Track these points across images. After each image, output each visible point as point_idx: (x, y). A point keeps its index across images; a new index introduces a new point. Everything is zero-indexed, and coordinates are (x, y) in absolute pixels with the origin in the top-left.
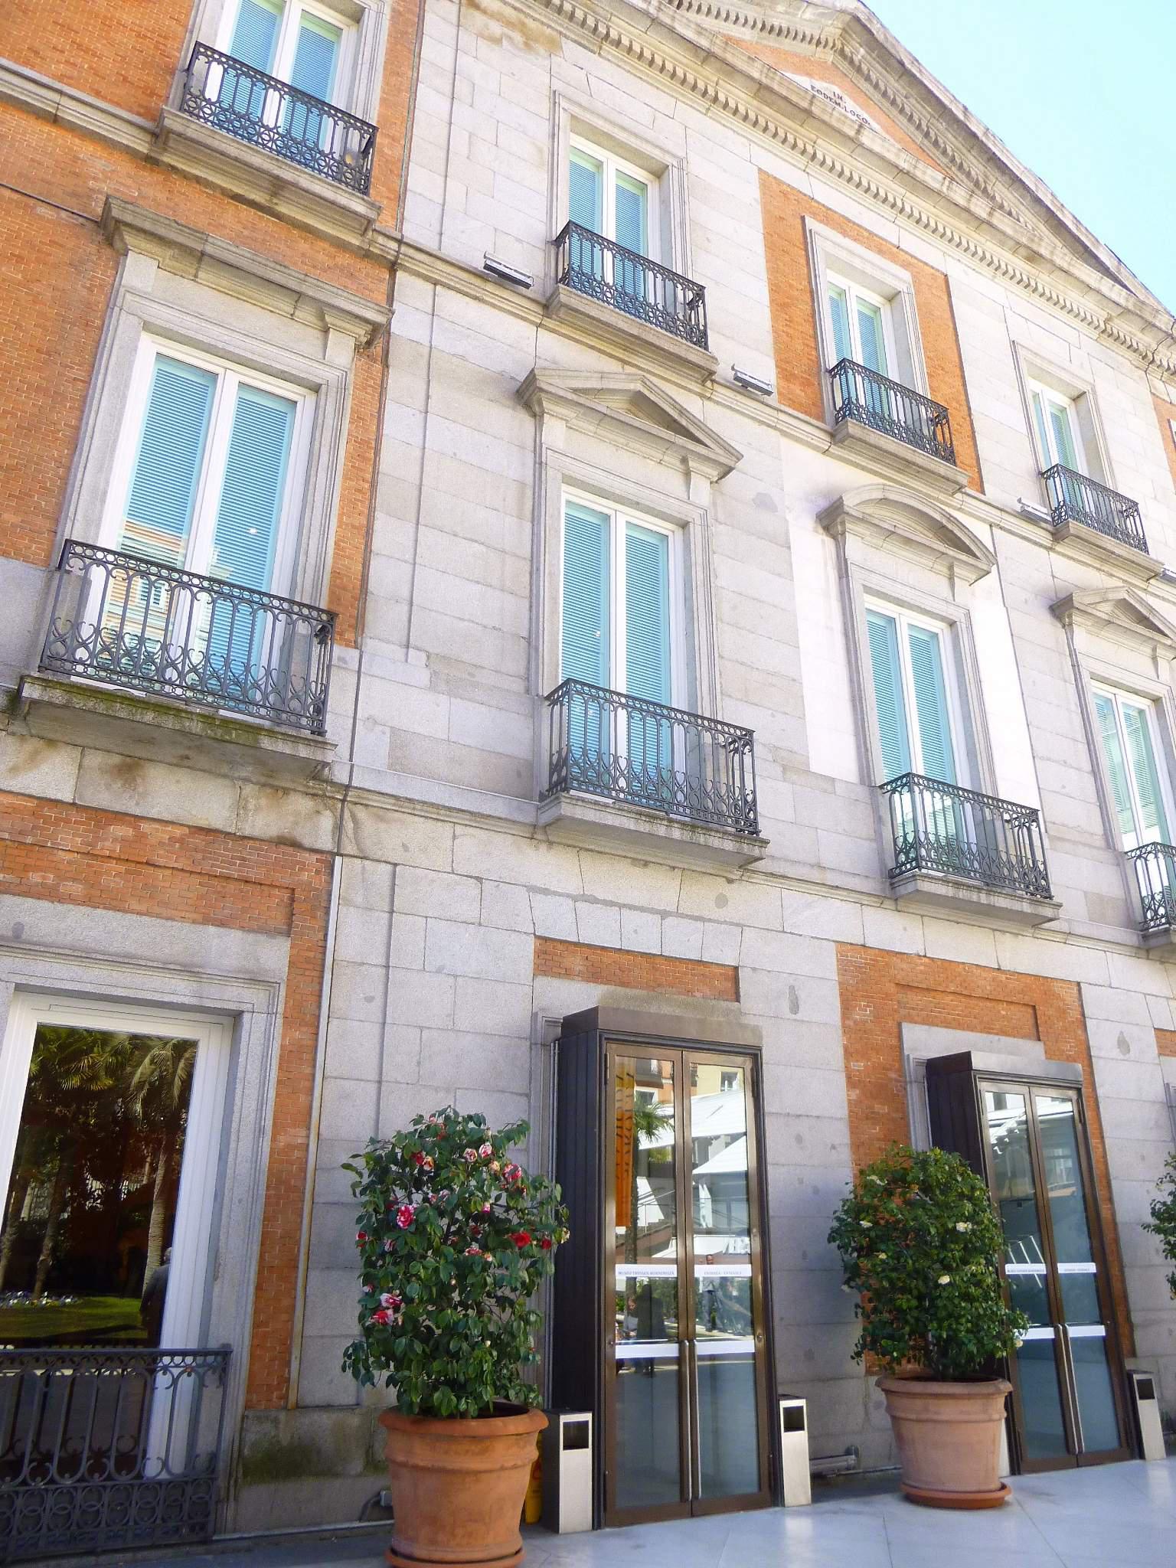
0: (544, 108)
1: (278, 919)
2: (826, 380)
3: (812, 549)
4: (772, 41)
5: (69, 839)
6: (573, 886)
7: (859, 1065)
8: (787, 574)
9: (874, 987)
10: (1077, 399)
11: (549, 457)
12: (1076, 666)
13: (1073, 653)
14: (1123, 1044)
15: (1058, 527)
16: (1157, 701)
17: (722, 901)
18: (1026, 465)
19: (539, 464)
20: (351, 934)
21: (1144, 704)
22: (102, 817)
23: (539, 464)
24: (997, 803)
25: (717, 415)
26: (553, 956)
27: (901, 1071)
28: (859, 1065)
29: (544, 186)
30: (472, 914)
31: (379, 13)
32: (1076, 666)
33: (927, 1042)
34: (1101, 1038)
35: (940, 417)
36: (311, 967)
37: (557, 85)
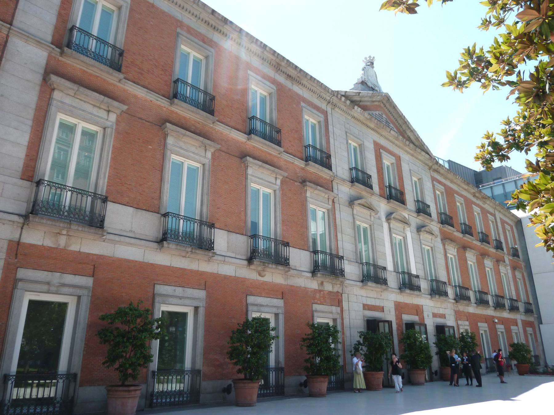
0: (345, 137)
1: (337, 305)
3: (385, 225)
5: (318, 296)
6: (365, 295)
8: (383, 232)
9: (400, 308)
10: (419, 179)
11: (355, 216)
12: (421, 243)
13: (420, 240)
14: (428, 316)
16: (432, 248)
17: (381, 295)
19: (354, 218)
21: (429, 248)
22: (320, 291)
23: (354, 218)
26: (366, 307)
29: (347, 156)
32: (421, 243)
36: (342, 311)
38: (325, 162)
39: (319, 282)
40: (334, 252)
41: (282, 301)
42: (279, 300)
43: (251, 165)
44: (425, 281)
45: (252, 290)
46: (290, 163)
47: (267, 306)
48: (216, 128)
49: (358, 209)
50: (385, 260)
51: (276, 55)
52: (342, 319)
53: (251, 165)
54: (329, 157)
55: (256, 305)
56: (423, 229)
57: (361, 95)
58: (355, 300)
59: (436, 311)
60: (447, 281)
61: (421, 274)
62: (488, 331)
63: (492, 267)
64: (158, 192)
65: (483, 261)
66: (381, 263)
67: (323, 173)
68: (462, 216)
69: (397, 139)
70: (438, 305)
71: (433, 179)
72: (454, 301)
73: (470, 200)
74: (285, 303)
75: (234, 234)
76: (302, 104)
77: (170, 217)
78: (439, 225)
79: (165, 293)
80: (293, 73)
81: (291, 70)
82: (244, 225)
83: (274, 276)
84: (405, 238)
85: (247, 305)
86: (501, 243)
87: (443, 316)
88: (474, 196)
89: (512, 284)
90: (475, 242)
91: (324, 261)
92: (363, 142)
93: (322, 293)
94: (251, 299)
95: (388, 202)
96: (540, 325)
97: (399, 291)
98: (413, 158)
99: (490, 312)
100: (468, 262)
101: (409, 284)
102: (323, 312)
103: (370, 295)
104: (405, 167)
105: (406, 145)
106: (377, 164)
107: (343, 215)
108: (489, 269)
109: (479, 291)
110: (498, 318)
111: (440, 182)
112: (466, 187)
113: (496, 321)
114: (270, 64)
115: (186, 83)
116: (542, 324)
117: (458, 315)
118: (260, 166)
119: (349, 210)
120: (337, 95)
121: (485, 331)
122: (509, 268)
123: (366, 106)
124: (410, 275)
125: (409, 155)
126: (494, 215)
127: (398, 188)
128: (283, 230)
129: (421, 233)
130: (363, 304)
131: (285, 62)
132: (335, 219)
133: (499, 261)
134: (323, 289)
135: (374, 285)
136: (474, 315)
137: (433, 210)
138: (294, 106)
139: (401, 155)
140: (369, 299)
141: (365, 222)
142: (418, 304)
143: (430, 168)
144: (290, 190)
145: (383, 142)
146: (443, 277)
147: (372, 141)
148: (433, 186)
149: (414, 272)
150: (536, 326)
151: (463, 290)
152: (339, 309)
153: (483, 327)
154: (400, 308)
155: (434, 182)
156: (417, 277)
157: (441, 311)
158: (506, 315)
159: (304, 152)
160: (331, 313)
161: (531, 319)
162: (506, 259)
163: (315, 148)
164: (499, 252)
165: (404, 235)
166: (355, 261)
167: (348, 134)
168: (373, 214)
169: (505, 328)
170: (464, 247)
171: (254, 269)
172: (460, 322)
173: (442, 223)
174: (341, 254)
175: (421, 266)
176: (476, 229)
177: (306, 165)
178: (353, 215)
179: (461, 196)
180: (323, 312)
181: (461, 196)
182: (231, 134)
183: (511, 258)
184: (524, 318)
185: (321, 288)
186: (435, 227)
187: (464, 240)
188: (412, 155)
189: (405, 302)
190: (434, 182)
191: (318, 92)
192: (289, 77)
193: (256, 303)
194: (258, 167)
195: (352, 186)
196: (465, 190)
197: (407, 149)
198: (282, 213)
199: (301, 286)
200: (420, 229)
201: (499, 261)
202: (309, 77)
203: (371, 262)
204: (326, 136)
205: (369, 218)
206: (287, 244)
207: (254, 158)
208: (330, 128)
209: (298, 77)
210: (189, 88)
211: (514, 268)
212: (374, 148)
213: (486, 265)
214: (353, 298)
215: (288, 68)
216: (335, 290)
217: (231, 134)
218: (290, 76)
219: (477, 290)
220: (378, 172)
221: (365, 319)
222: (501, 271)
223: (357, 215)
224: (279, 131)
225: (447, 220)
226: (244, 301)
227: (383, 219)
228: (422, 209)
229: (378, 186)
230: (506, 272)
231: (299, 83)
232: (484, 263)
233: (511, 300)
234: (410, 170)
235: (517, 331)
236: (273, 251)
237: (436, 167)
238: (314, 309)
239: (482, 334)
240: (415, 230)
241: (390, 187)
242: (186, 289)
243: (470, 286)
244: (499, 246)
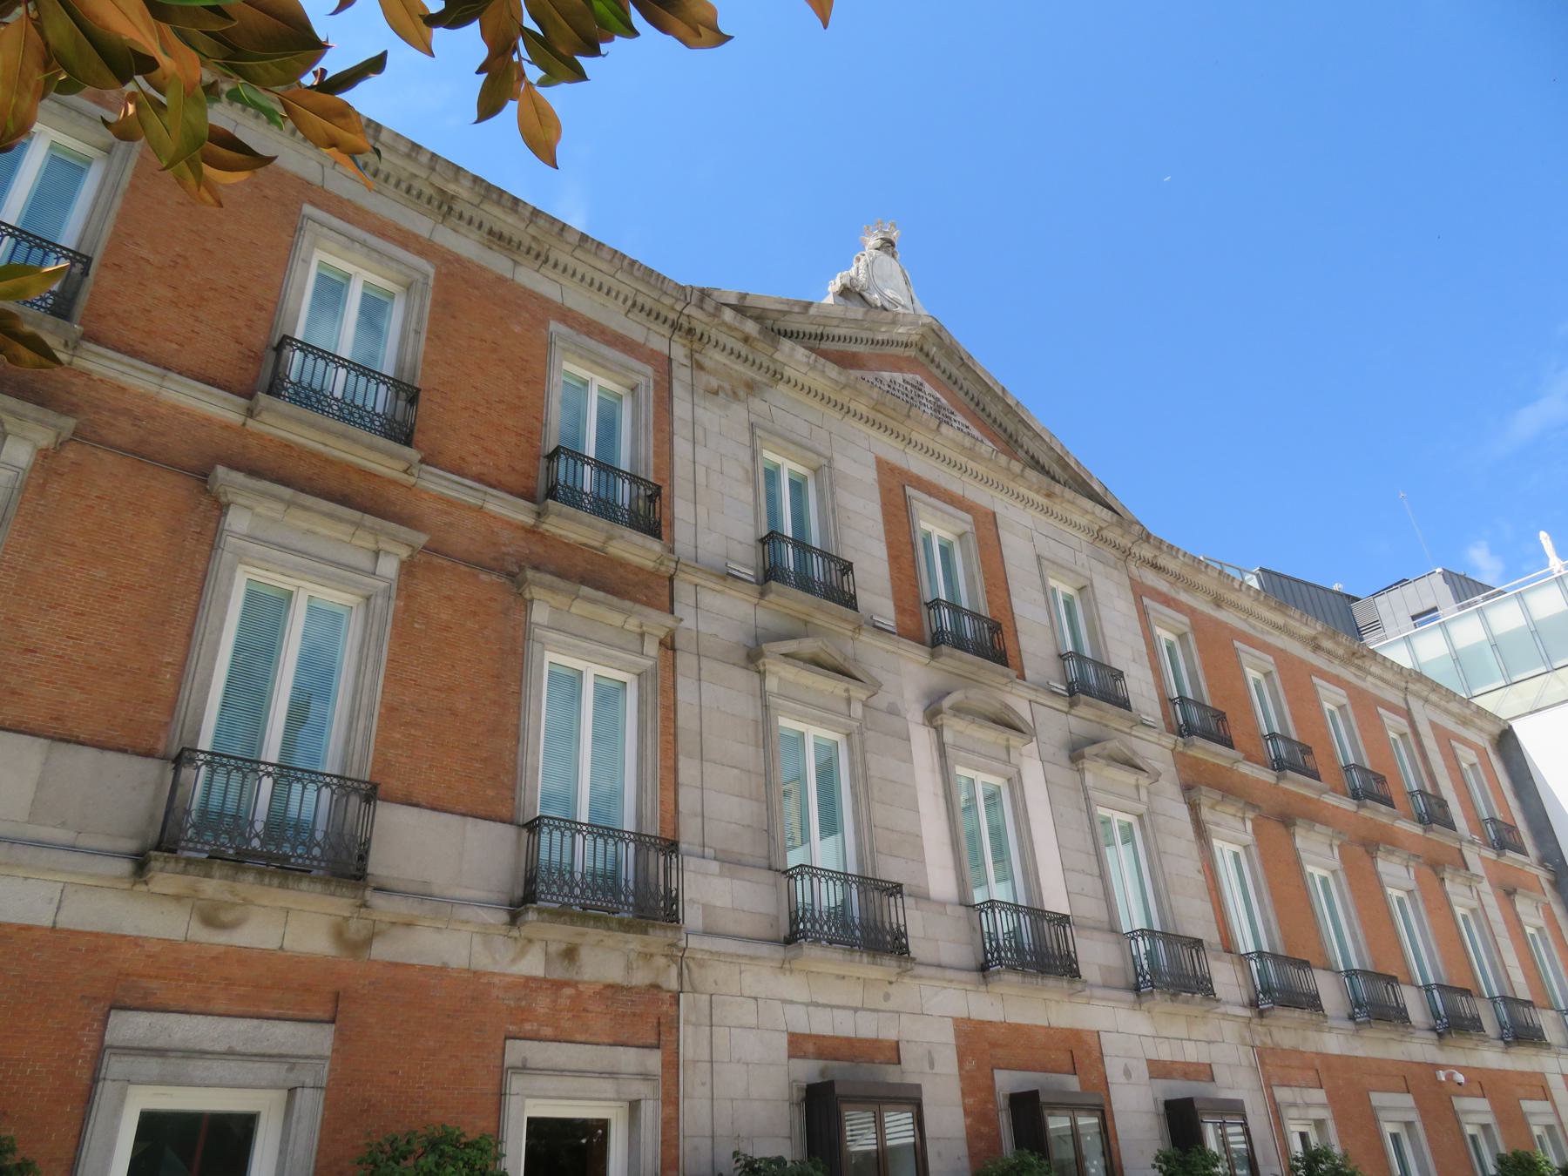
0: (746, 438)
2: (924, 610)
3: (922, 738)
4: (878, 350)
5: (542, 1004)
6: (805, 998)
7: (970, 1101)
8: (908, 759)
9: (977, 1043)
10: (1081, 590)
12: (1087, 799)
13: (1085, 789)
14: (1127, 1073)
15: (1075, 691)
16: (1140, 817)
17: (887, 997)
18: (1048, 650)
20: (691, 1042)
22: (558, 985)
26: (798, 1045)
27: (995, 1102)
28: (970, 1101)
29: (751, 499)
30: (752, 1021)
31: (648, 387)
33: (1007, 1082)
34: (1114, 1069)
35: (996, 628)
36: (672, 1065)
37: (753, 418)
38: (650, 515)
39: (553, 948)
43: (240, 500)
44: (1111, 937)
45: (154, 984)
46: (470, 507)
47: (230, 1054)
48: (89, 366)
49: (780, 674)
51: (424, 159)
53: (240, 500)
55: (160, 1053)
56: (1088, 750)
57: (812, 311)
58: (751, 1020)
59: (1165, 1053)
60: (1210, 935)
62: (1419, 1126)
63: (1412, 885)
65: (1374, 866)
66: (891, 870)
67: (634, 549)
68: (1268, 712)
69: (971, 453)
70: (1178, 1028)
71: (1140, 592)
72: (1247, 1013)
73: (1302, 662)
74: (341, 1039)
75: (89, 754)
76: (554, 326)
78: (1169, 740)
80: (507, 223)
81: (497, 211)
83: (291, 924)
84: (1015, 783)
86: (1443, 804)
88: (1317, 648)
89: (1505, 943)
90: (1329, 799)
92: (830, 460)
93: (568, 991)
95: (933, 656)
97: (975, 976)
98: (1051, 520)
99: (1420, 1049)
100: (1389, 891)
101: (1038, 950)
102: (560, 1072)
103: (836, 999)
104: (1017, 550)
105: (1015, 477)
106: (888, 532)
107: (713, 699)
108: (1401, 894)
109: (1440, 987)
111: (1168, 601)
112: (1279, 619)
114: (408, 191)
117: (1275, 1066)
118: (290, 504)
119: (743, 678)
120: (702, 300)
121: (1485, 1127)
122: (1485, 887)
123: (854, 355)
125: (1031, 511)
126: (1408, 714)
129: (1087, 764)
131: (467, 183)
133: (1437, 866)
134: (571, 975)
135: (1013, 978)
136: (1347, 1062)
137: (1139, 685)
139: (999, 509)
141: (821, 722)
142: (1078, 1026)
143: (1127, 553)
145: (917, 464)
146: (1195, 920)
147: (872, 461)
148: (1143, 614)
149: (1056, 902)
151: (1292, 972)
152: (654, 1061)
153: (1395, 1111)
154: (977, 1043)
155: (1146, 601)
157: (1192, 1053)
158: (1491, 1057)
160: (612, 1075)
162: (1471, 855)
164: (1438, 835)
165: (1012, 771)
166: (764, 863)
167: (758, 432)
168: (858, 693)
169: (1497, 1109)
170: (1282, 819)
171: (177, 898)
172: (1282, 1094)
173: (1185, 731)
176: (1332, 755)
177: (250, 413)
178: (763, 694)
179: (1265, 647)
180: (560, 1072)
181: (1265, 647)
182: (164, 392)
183: (1490, 854)
185: (559, 973)
186: (1156, 749)
187: (1286, 791)
188: (1047, 511)
189: (1012, 1019)
190: (1146, 601)
191: (625, 290)
192: (497, 238)
193: (160, 1043)
194: (281, 507)
195: (762, 595)
196: (1276, 627)
197: (1023, 491)
199: (444, 969)
200: (1076, 752)
201: (1437, 866)
202: (575, 239)
204: (658, 429)
205: (843, 708)
207: (254, 472)
209: (534, 238)
211: (1508, 894)
212: (880, 482)
213: (1385, 878)
215: (486, 206)
216: (641, 978)
217: (164, 392)
218: (501, 237)
219: (1432, 981)
220: (894, 558)
222: (1454, 898)
223: (779, 695)
225: (1203, 722)
227: (914, 713)
228: (1090, 683)
230: (1475, 904)
231: (541, 258)
232: (1377, 874)
233: (1510, 1001)
234: (1039, 557)
235: (1552, 1120)
237: (1147, 552)
239: (1473, 1137)
240: (1063, 757)
243: (1408, 972)
244: (1434, 814)
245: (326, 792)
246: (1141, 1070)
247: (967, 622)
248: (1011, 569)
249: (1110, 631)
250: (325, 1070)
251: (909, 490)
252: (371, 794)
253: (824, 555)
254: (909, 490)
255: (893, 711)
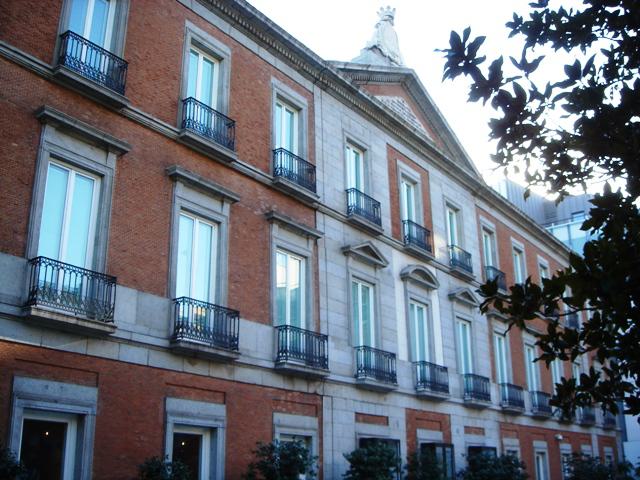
3: (399, 286)
8: (394, 297)
9: (415, 420)
14: (458, 431)
20: (326, 414)
24: (435, 365)
25: (382, 248)
26: (361, 417)
30: (344, 407)
33: (425, 435)
36: (321, 423)
37: (344, 126)
40: (313, 329)
41: (224, 406)
42: (219, 406)
50: (395, 341)
52: (321, 437)
54: (312, 169)
55: (182, 415)
59: (470, 424)
61: (450, 364)
62: (547, 454)
64: (24, 222)
66: (387, 347)
74: (229, 411)
77: (43, 264)
79: (30, 390)
82: (165, 280)
85: (165, 413)
87: (480, 431)
91: (295, 343)
94: (173, 404)
96: (625, 444)
106: (390, 184)
110: (561, 432)
111: (488, 216)
113: (560, 437)
115: (80, 38)
116: (626, 440)
124: (433, 366)
127: (423, 225)
128: (231, 291)
130: (357, 413)
132: (317, 274)
138: (260, 82)
140: (365, 405)
144: (245, 223)
148: (479, 222)
149: (440, 362)
150: (618, 444)
155: (481, 217)
156: (445, 369)
157: (479, 424)
159: (272, 160)
161: (613, 434)
163: (291, 154)
174: (323, 331)
175: (451, 353)
184: (601, 432)
190: (481, 217)
198: (231, 262)
203: (373, 345)
204: (310, 134)
206: (235, 314)
208: (318, 121)
210: (85, 47)
212: (388, 157)
214: (338, 403)
220: (392, 197)
221: (358, 437)
224: (231, 124)
226: (161, 407)
229: (390, 221)
236: (212, 326)
238: (275, 420)
241: (410, 221)
242: (65, 385)
243: (525, 384)
245: (85, 278)
246: (462, 430)
247: (414, 229)
248: (433, 201)
249: (467, 233)
250: (225, 423)
251: (399, 163)
252: (112, 280)
253: (367, 197)
254: (399, 163)
255: (390, 273)
